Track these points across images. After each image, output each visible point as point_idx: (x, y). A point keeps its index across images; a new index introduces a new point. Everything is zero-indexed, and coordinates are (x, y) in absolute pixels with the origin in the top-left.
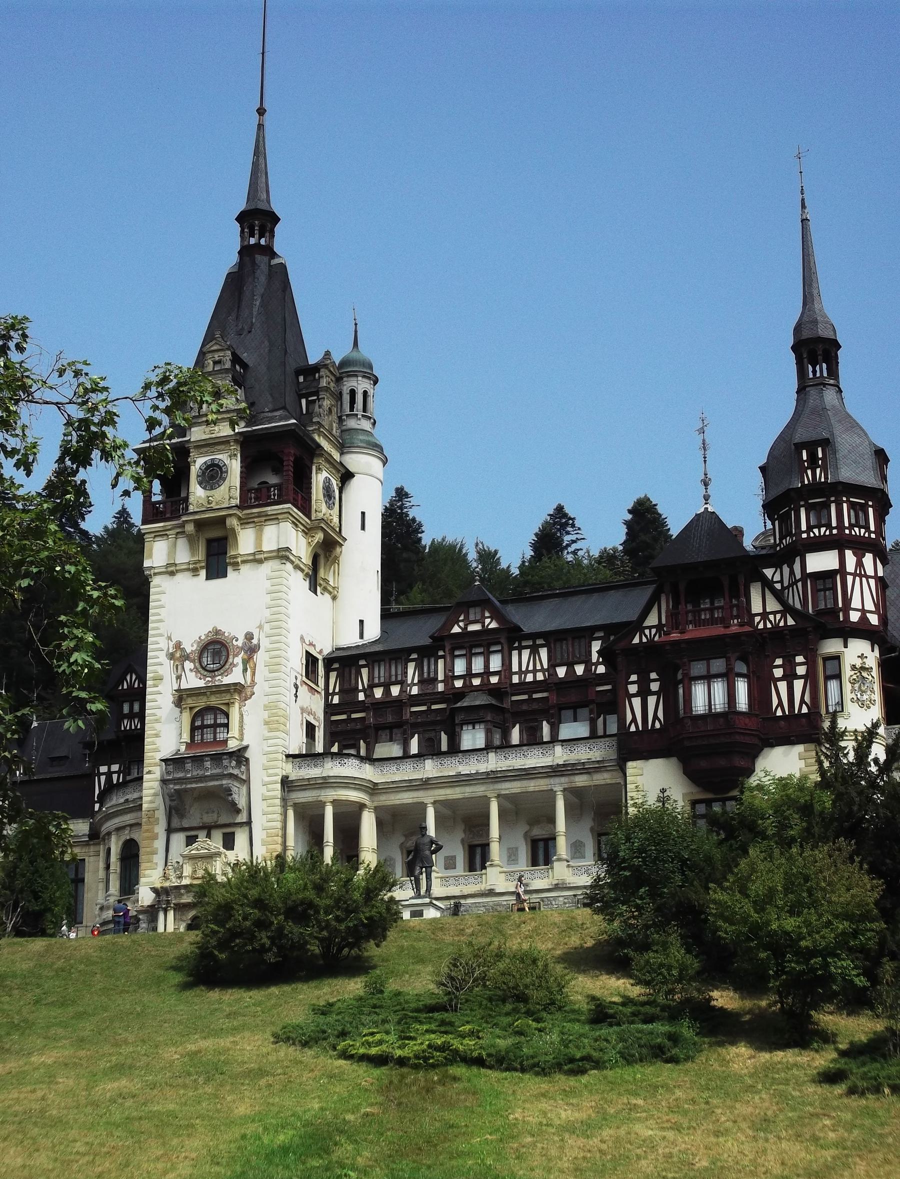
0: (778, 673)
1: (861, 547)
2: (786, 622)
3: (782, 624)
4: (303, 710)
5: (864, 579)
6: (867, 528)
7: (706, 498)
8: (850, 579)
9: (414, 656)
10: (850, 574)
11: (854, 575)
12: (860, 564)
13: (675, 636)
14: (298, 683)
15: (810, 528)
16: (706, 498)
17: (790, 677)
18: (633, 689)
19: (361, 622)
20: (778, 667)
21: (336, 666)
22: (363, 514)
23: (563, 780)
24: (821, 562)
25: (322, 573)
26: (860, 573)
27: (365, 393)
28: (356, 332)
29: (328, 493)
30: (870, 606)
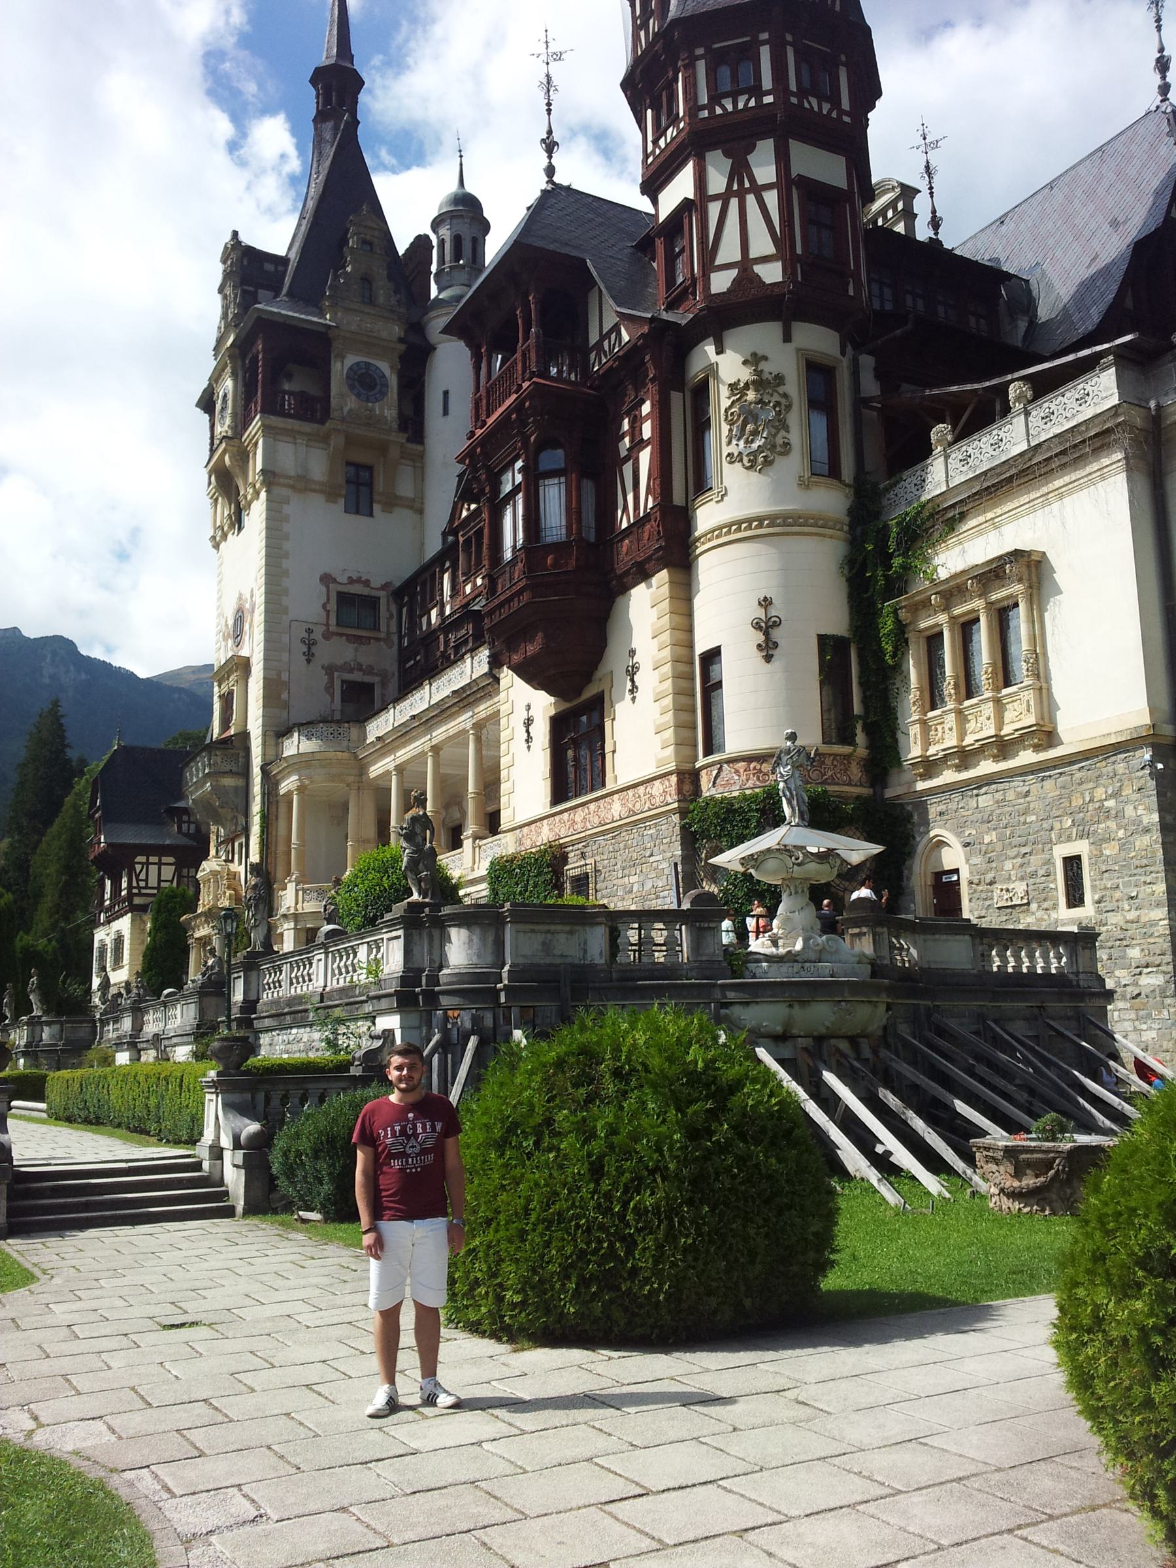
4: (330, 670)
5: (751, 199)
7: (550, 171)
8: (714, 209)
9: (447, 564)
10: (715, 198)
11: (725, 198)
12: (740, 170)
15: (655, 142)
16: (550, 171)
21: (406, 599)
22: (446, 393)
25: (380, 485)
27: (457, 240)
28: (461, 165)
29: (365, 382)
30: (761, 244)
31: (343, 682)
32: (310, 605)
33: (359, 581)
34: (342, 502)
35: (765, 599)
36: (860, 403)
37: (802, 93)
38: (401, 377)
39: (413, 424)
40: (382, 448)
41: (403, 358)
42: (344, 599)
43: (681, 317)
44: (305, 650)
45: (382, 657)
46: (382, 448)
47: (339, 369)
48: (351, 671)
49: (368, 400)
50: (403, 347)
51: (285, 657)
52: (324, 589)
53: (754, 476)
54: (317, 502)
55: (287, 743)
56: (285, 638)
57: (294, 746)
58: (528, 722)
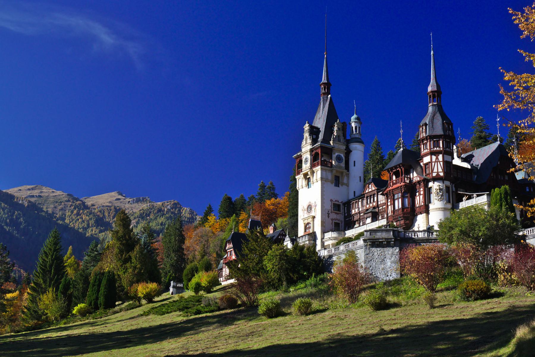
0: (417, 194)
1: (436, 153)
4: (332, 220)
6: (440, 147)
8: (433, 164)
11: (435, 162)
12: (437, 158)
13: (391, 188)
14: (330, 212)
17: (420, 194)
18: (389, 204)
19: (354, 192)
22: (355, 162)
24: (427, 159)
25: (340, 181)
26: (437, 161)
27: (356, 127)
29: (339, 159)
30: (440, 170)
32: (329, 206)
36: (453, 192)
37: (446, 148)
39: (347, 167)
40: (342, 173)
41: (346, 153)
43: (428, 177)
45: (340, 217)
46: (342, 173)
47: (334, 156)
54: (330, 183)
55: (325, 234)
57: (328, 235)
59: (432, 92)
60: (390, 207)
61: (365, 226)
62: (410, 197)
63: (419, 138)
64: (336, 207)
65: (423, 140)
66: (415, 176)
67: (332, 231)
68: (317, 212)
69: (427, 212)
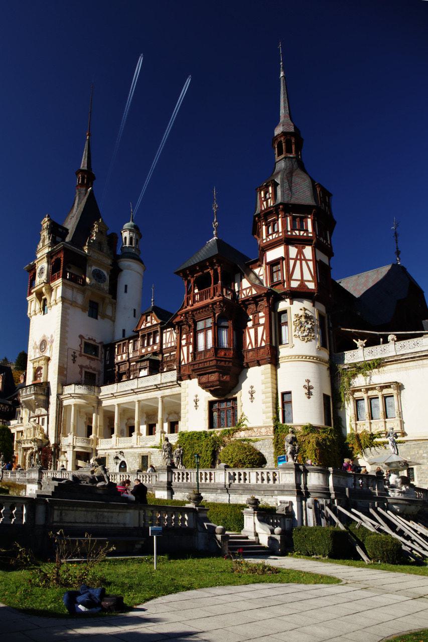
0: (250, 324)
2: (252, 293)
3: (250, 294)
4: (81, 367)
14: (77, 354)
17: (256, 325)
18: (184, 342)
20: (250, 320)
23: (159, 392)
27: (131, 238)
31: (86, 372)
33: (92, 339)
34: (87, 312)
35: (308, 380)
38: (110, 277)
40: (103, 299)
41: (111, 271)
42: (86, 344)
44: (72, 358)
45: (96, 365)
48: (88, 368)
49: (99, 282)
50: (111, 268)
51: (66, 360)
52: (80, 340)
53: (304, 342)
56: (66, 354)
58: (196, 401)
59: (284, 134)
60: (185, 349)
61: (135, 380)
62: (234, 329)
63: (258, 211)
64: (90, 348)
65: (268, 213)
66: (245, 287)
67: (77, 384)
68: (54, 352)
69: (275, 361)
